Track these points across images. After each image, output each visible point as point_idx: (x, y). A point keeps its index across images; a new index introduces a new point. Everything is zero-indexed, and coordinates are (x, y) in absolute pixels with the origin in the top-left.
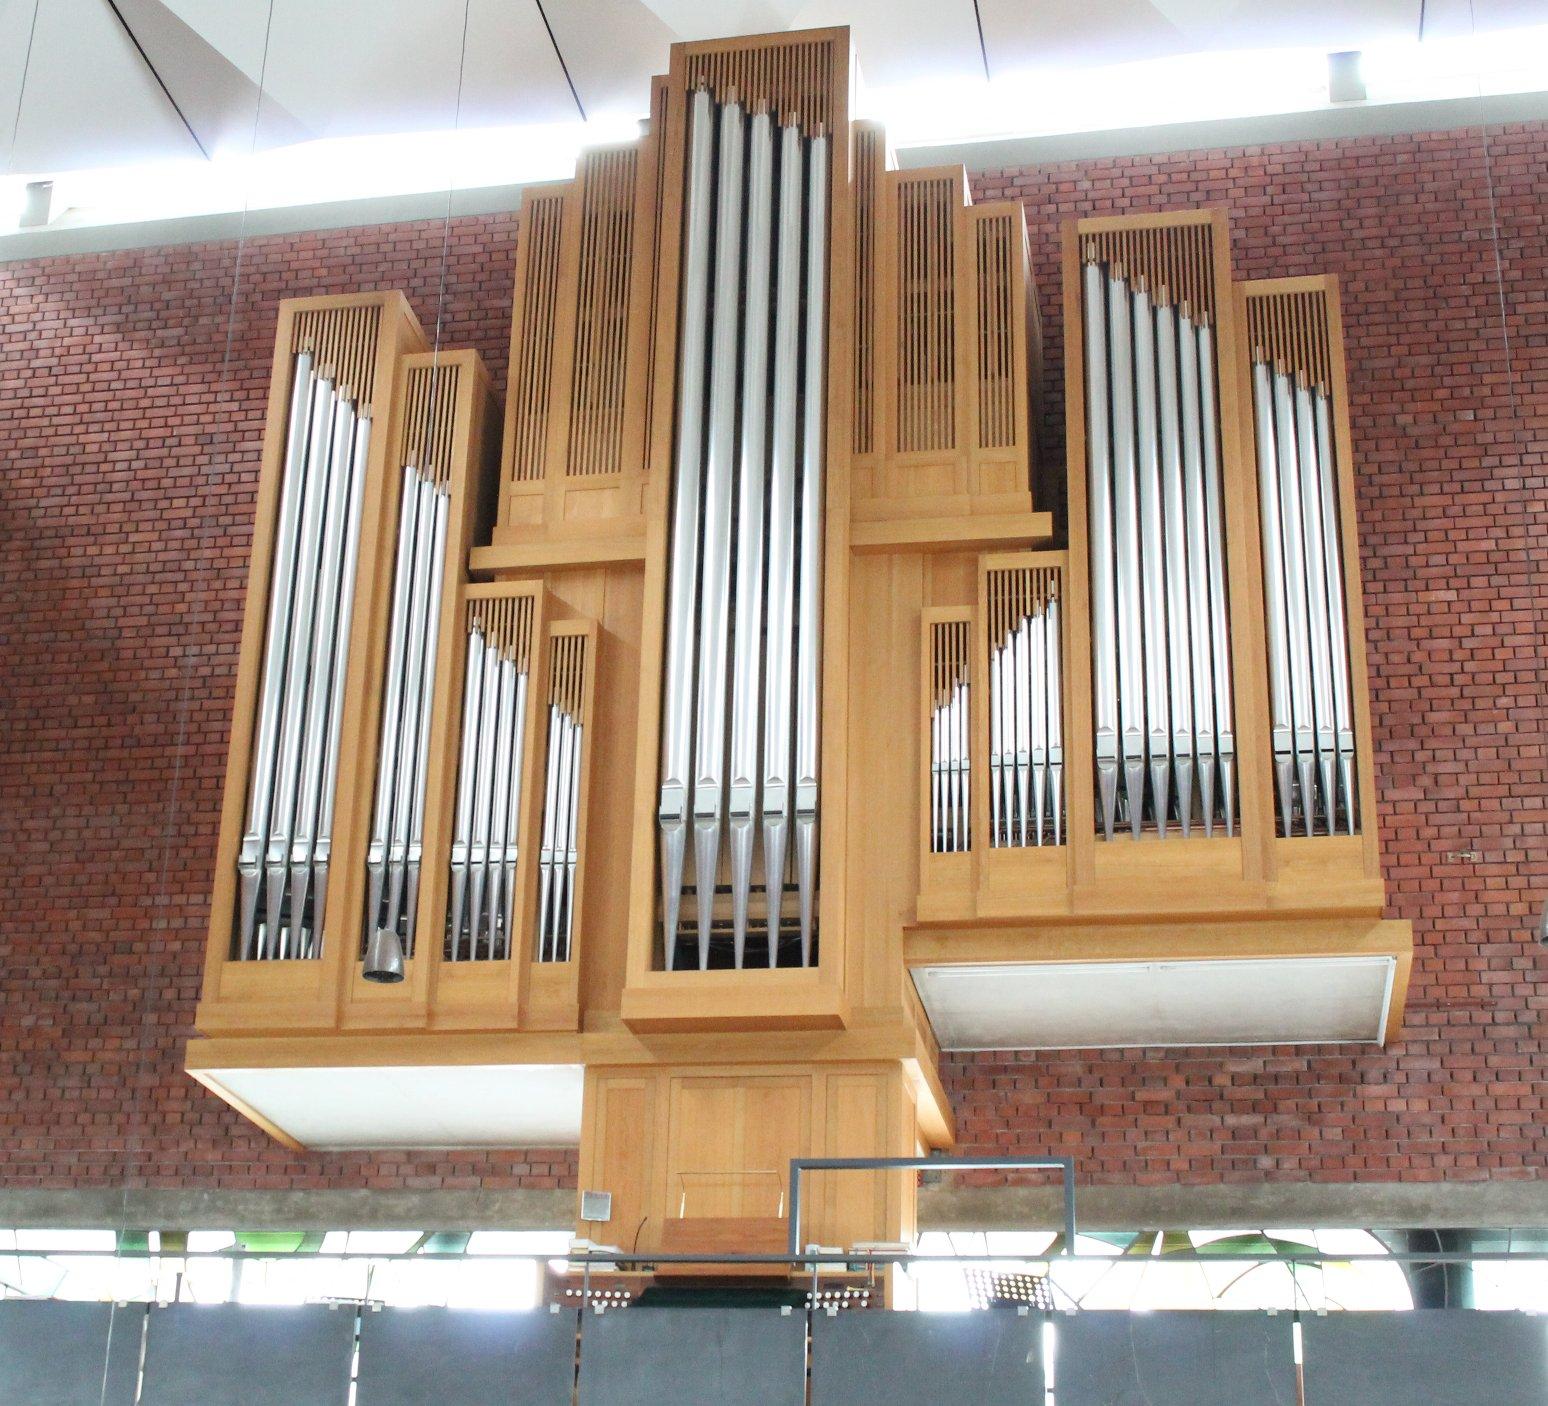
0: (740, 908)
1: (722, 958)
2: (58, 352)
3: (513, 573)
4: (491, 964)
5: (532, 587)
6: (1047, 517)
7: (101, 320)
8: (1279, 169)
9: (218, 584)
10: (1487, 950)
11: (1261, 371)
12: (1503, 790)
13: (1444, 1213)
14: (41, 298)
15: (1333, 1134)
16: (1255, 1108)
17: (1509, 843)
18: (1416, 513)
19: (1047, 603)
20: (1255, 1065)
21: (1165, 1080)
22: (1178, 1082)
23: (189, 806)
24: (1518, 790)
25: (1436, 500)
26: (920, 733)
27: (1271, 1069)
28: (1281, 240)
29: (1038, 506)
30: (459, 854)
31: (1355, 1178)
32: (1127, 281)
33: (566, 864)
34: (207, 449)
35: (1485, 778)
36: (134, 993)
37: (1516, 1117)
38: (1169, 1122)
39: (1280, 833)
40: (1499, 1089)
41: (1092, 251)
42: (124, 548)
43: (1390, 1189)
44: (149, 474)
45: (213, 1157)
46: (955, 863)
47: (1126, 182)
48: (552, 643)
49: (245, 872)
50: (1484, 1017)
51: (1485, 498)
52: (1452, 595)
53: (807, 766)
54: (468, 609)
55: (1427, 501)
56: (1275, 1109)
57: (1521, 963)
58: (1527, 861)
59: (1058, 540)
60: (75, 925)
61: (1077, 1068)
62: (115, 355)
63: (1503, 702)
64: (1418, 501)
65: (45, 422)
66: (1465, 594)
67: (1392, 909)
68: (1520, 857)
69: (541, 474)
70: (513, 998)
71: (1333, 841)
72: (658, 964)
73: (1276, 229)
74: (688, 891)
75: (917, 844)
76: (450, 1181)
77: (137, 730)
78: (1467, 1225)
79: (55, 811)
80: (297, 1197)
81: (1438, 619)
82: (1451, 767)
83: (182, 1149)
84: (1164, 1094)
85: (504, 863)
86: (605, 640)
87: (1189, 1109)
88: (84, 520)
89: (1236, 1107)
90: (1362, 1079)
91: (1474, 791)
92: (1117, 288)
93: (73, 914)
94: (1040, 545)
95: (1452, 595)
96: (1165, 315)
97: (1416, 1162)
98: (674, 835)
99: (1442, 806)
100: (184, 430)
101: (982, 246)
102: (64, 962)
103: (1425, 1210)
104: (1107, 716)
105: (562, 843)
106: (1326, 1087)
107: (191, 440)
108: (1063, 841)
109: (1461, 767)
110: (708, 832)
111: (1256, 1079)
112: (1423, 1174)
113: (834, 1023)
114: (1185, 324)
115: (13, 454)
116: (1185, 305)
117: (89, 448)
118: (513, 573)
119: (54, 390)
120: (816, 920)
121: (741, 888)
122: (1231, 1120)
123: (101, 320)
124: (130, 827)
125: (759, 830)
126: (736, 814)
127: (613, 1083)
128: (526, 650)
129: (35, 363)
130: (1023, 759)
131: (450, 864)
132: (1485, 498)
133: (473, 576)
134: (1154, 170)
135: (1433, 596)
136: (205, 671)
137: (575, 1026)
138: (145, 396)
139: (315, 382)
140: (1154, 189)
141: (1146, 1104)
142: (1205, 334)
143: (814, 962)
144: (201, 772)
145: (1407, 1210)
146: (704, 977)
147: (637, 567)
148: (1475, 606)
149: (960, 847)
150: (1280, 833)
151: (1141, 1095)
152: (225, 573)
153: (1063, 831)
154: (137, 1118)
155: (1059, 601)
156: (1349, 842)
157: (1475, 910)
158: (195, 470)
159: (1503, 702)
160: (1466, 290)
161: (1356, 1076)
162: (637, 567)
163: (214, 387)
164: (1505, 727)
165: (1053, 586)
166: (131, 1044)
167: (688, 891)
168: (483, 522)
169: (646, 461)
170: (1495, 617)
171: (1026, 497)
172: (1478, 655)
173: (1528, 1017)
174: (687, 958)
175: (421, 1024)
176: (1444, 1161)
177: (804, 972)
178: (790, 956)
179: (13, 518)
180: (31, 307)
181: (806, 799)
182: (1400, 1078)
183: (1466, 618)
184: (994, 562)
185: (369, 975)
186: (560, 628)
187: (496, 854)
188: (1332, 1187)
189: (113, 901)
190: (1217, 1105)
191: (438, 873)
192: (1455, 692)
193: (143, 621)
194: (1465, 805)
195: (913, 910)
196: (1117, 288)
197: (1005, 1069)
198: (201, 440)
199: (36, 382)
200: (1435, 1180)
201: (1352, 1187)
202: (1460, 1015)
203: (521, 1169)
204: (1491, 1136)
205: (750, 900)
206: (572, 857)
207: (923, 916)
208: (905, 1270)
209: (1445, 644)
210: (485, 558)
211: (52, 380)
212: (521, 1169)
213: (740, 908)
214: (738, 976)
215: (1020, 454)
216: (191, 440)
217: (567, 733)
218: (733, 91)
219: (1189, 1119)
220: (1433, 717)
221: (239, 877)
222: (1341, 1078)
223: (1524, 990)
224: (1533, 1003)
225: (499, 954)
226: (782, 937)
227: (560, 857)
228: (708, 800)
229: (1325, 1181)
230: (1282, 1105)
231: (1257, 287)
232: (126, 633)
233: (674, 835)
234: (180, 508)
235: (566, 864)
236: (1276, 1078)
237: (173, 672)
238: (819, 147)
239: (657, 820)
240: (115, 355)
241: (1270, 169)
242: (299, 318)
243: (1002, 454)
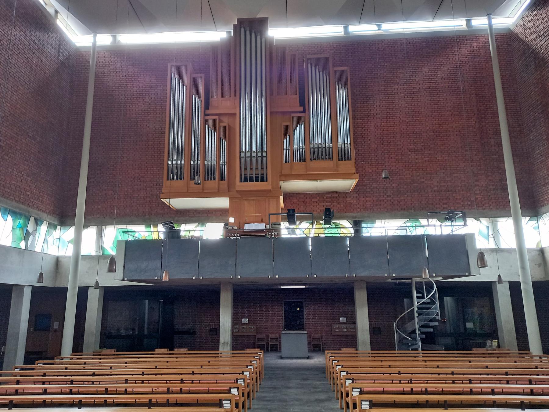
0: (254, 172)
1: (251, 180)
2: (121, 68)
3: (213, 115)
4: (213, 181)
5: (217, 117)
6: (302, 107)
7: (129, 63)
8: (335, 46)
9: (155, 113)
10: (366, 177)
11: (337, 83)
12: (368, 152)
13: (359, 218)
14: (116, 58)
15: (342, 206)
16: (330, 202)
17: (369, 161)
18: (356, 107)
19: (302, 122)
20: (330, 195)
21: (316, 197)
22: (318, 198)
23: (153, 153)
24: (371, 152)
25: (360, 105)
26: (283, 144)
27: (333, 196)
28: (336, 59)
29: (300, 106)
30: (206, 162)
31: (345, 213)
32: (315, 67)
33: (224, 164)
34: (151, 88)
35: (366, 150)
36: (145, 185)
37: (369, 203)
38: (317, 204)
39: (339, 160)
40: (367, 199)
41: (309, 61)
42: (137, 106)
43: (351, 214)
44: (140, 93)
45: (161, 212)
46: (287, 165)
47: (310, 48)
48: (220, 127)
49: (169, 165)
50: (365, 188)
51: (367, 104)
52: (361, 121)
53: (264, 149)
55: (358, 105)
56: (333, 202)
57: (371, 179)
58: (372, 163)
59: (304, 112)
60: (133, 173)
61: (303, 196)
62: (132, 70)
63: (369, 138)
64: (357, 105)
65: (120, 82)
66: (363, 121)
67: (357, 173)
68: (371, 163)
70: (217, 187)
71: (347, 162)
73: (335, 57)
74: (246, 169)
75: (282, 162)
76: (202, 215)
77: (142, 139)
78: (362, 220)
79: (128, 153)
80: (176, 218)
81: (359, 125)
82: (361, 148)
83: (156, 210)
84: (317, 200)
85: (214, 164)
86: (230, 127)
87: (320, 202)
88: (129, 101)
89: (327, 202)
90: (346, 198)
91: (364, 152)
92: (313, 68)
93: (133, 171)
94: (300, 112)
95: (361, 121)
96: (321, 73)
97: (355, 210)
98: (243, 160)
99: (359, 155)
100: (146, 85)
101: (291, 60)
102: (132, 179)
103: (356, 217)
104: (312, 141)
105: (223, 161)
106: (341, 199)
107: (148, 87)
108: (305, 161)
109: (362, 149)
110: (248, 159)
111: (330, 197)
112: (355, 212)
113: (270, 191)
115: (114, 88)
116: (325, 71)
117: (129, 87)
118: (213, 115)
119: (121, 76)
120: (267, 175)
121: (254, 169)
122: (326, 204)
123: (129, 63)
124: (142, 156)
125: (257, 159)
126: (253, 157)
127: (234, 200)
128: (216, 128)
129: (117, 70)
130: (298, 148)
131: (205, 164)
132: (367, 104)
133: (206, 115)
134: (315, 46)
135: (359, 121)
136: (154, 129)
137: (227, 191)
138: (139, 78)
139: (175, 79)
140: (315, 49)
141: (313, 201)
143: (267, 181)
144: (155, 147)
145: (353, 217)
146: (249, 183)
147: (235, 114)
148: (365, 122)
149: (289, 162)
150: (339, 160)
151: (313, 200)
152: (156, 111)
153: (305, 160)
154: (147, 206)
155: (304, 122)
156: (350, 162)
157: (364, 171)
158: (149, 92)
159: (369, 138)
160: (365, 69)
161: (345, 197)
162: (235, 114)
163: (152, 77)
164: (369, 142)
165: (303, 119)
166: (145, 193)
167: (246, 169)
168: (207, 105)
169: (235, 96)
170: (368, 124)
171: (299, 104)
172: (365, 130)
173: (372, 188)
174: (246, 180)
175: (202, 191)
176: (359, 210)
177: (265, 183)
178: (262, 180)
179: (115, 100)
180: (115, 60)
181: (264, 154)
182: (352, 197)
183: (364, 124)
185: (195, 184)
186: (222, 124)
187: (213, 163)
188: (342, 214)
189: (140, 169)
190: (324, 202)
191: (203, 165)
192: (361, 136)
193: (142, 119)
194: (363, 155)
195: (281, 172)
196: (313, 68)
197: (291, 196)
198: (150, 87)
199: (117, 74)
200: (358, 213)
201: (345, 214)
202: (361, 187)
203: (214, 213)
204: (366, 206)
205: (256, 171)
206: (225, 163)
207: (283, 173)
208: (499, 276)
209: (360, 128)
210: (208, 112)
211: (120, 74)
212: (214, 213)
213: (254, 172)
214: (254, 183)
215: (297, 96)
216: (148, 87)
217: (224, 142)
218: (248, 29)
219: (320, 204)
220: (358, 140)
221: (168, 166)
222: (343, 197)
223: (371, 184)
224: (373, 186)
225: (214, 179)
226: (261, 177)
227: (223, 163)
228: (248, 154)
229: (341, 213)
230: (334, 202)
232: (139, 122)
233: (243, 160)
234: (147, 100)
235: (224, 164)
236: (333, 197)
237: (148, 129)
238: (258, 37)
239: (240, 157)
240: (132, 70)
241: (334, 46)
242: (172, 66)
243: (295, 96)
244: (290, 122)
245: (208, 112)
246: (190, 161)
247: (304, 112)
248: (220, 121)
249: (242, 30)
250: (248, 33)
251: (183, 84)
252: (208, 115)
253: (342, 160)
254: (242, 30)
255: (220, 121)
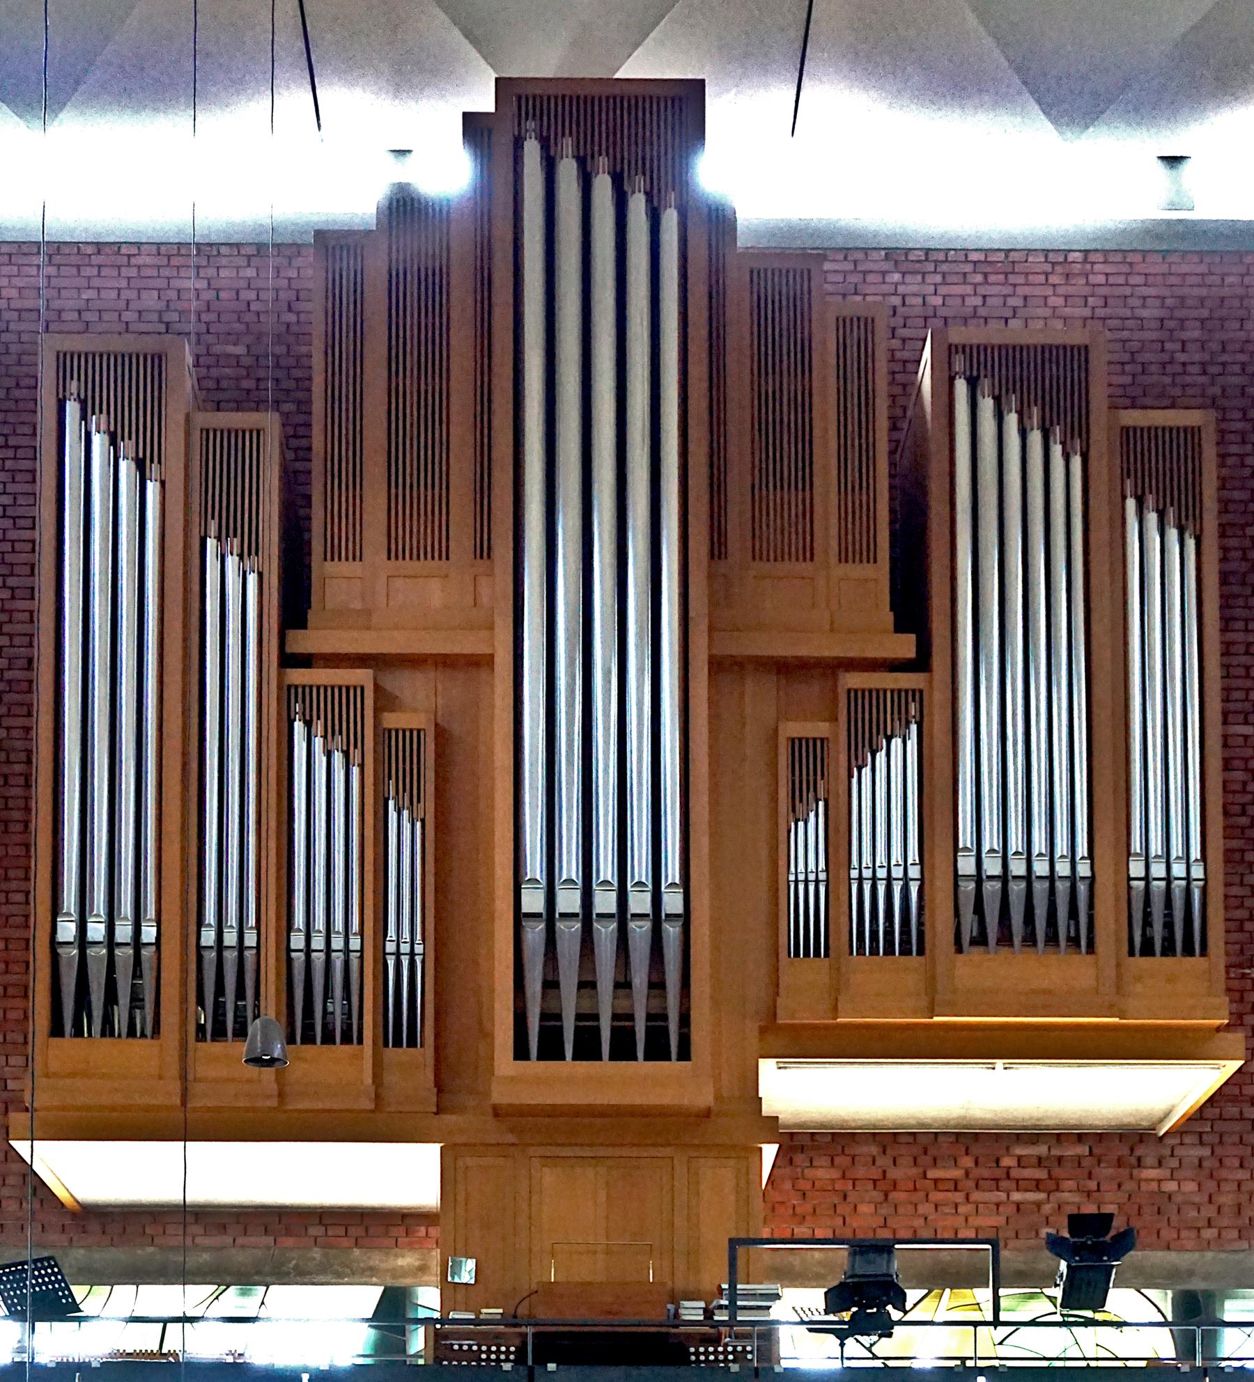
4: (340, 1050)
5: (362, 676)
11: (1131, 504)
19: (908, 723)
29: (900, 628)
30: (297, 941)
33: (412, 954)
41: (959, 363)
48: (384, 735)
53: (672, 870)
54: (288, 693)
59: (921, 662)
69: (358, 556)
72: (521, 1052)
74: (551, 985)
96: (1036, 437)
98: (535, 933)
101: (842, 347)
113: (707, 1114)
114: (1057, 450)
120: (685, 1020)
128: (359, 742)
131: (289, 950)
133: (288, 660)
142: (1077, 462)
143: (684, 1055)
167: (551, 985)
169: (483, 551)
171: (889, 617)
174: (551, 1049)
177: (673, 1067)
178: (657, 1051)
181: (673, 902)
184: (854, 680)
196: (987, 405)
206: (419, 949)
210: (302, 642)
215: (880, 572)
217: (407, 826)
227: (405, 948)
231: (1133, 418)
235: (412, 954)
239: (519, 917)
242: (63, 360)
243: (866, 570)
244: (834, 719)
245: (302, 642)
246: (193, 928)
247: (921, 662)
248: (385, 701)
249: (532, 149)
250: (568, 170)
251: (140, 465)
252: (306, 661)
253: (1147, 950)
254: (532, 149)
255: (385, 701)
